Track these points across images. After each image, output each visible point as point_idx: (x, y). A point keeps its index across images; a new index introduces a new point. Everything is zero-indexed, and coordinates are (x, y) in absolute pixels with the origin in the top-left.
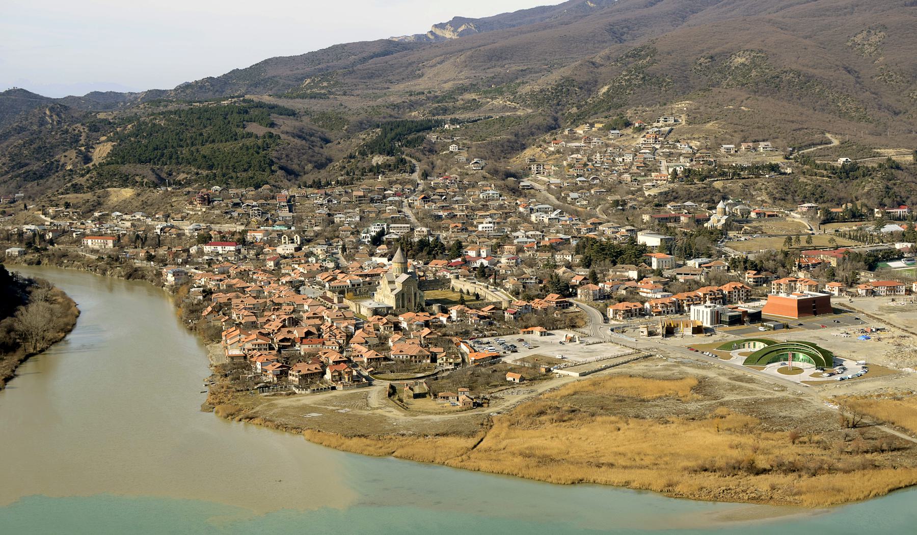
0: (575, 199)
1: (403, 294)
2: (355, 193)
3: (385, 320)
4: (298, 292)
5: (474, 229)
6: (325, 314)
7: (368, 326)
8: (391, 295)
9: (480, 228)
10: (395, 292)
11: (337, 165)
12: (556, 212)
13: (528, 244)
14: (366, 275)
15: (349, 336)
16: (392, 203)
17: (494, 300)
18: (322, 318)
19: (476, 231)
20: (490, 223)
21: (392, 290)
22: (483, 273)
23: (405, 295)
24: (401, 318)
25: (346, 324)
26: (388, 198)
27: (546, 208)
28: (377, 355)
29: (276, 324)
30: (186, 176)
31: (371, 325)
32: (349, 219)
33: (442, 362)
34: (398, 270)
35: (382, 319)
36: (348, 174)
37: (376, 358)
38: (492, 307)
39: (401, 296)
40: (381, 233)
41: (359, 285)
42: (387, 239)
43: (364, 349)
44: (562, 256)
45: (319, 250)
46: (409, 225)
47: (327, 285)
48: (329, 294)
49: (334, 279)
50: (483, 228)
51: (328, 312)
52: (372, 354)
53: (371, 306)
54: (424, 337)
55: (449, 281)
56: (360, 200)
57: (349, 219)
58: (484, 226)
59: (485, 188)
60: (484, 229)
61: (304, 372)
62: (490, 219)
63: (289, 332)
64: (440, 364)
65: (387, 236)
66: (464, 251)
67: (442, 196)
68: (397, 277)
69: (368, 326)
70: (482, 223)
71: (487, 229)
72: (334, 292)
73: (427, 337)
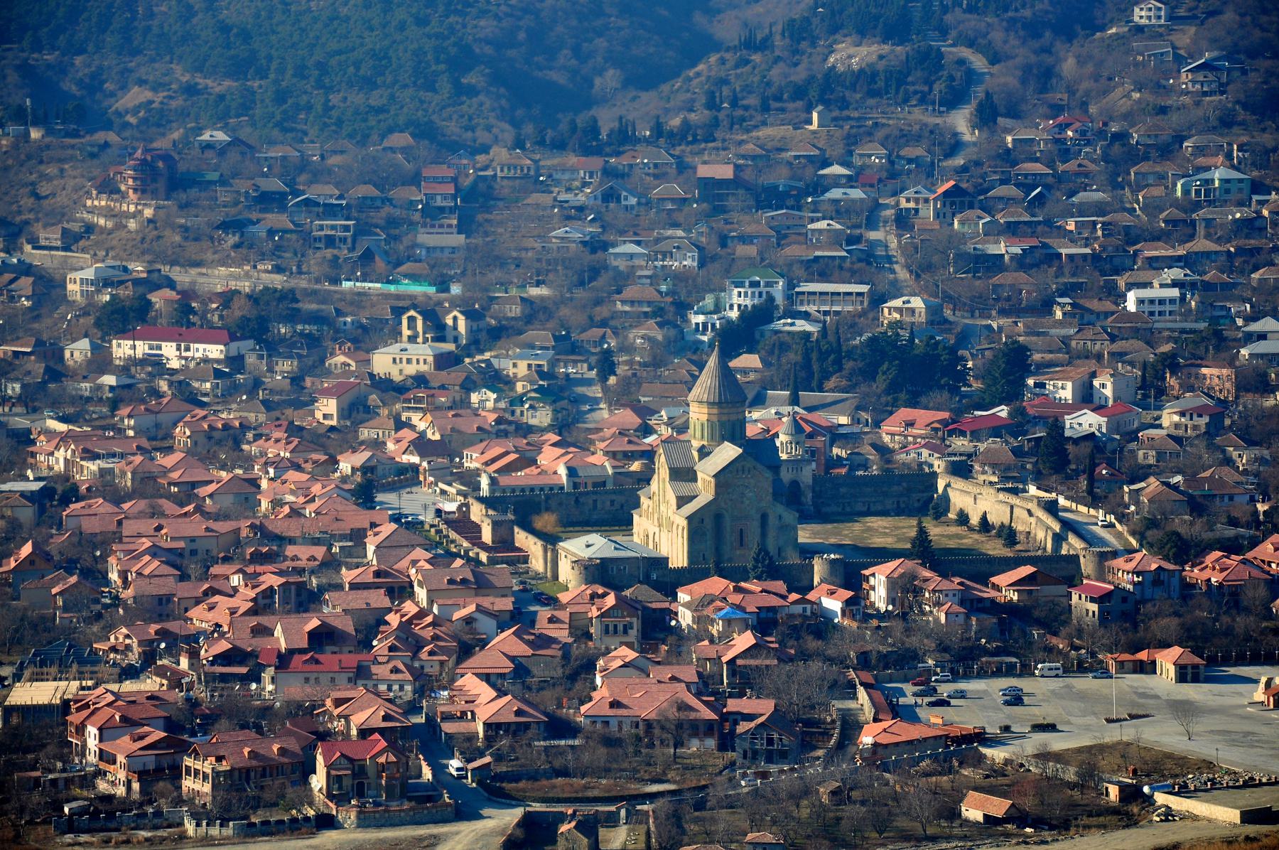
1: (718, 518)
2: (704, 171)
11: (698, 74)
23: (727, 523)
30: (148, 95)
39: (709, 524)
60: (1147, 308)
71: (1157, 308)
73: (739, 662)
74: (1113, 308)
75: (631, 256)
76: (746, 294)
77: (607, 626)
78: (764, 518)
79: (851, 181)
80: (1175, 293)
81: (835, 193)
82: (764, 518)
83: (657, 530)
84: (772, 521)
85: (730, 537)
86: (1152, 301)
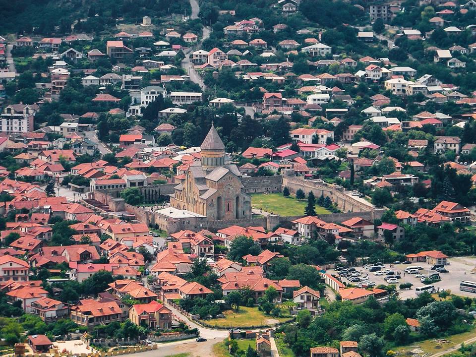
0: (448, 59)
1: (219, 198)
3: (200, 237)
4: (50, 191)
5: (300, 101)
6: (104, 226)
7: (174, 246)
8: (199, 200)
9: (310, 100)
10: (205, 196)
12: (422, 79)
13: (390, 128)
14: (149, 170)
15: (149, 258)
16: (166, 60)
17: (356, 210)
18: (98, 232)
19: (303, 105)
20: (323, 92)
21: (202, 192)
22: (328, 170)
24: (221, 235)
25: (140, 243)
26: (160, 52)
27: (406, 72)
28: (201, 290)
29: (27, 242)
31: (179, 244)
32: (104, 84)
33: (302, 301)
34: (210, 162)
35: (193, 235)
36: (91, 14)
37: (200, 295)
38: (358, 219)
39: (215, 202)
40: (160, 103)
41: (141, 183)
42: (167, 113)
43: (180, 282)
44: (444, 145)
45: (65, 131)
46: (200, 94)
47: (93, 183)
48: (99, 197)
49: (101, 174)
50: (315, 100)
51: (107, 224)
52: (193, 288)
53: (172, 216)
54: (266, 263)
55: (279, 179)
56: (118, 54)
57: (104, 84)
58: (317, 95)
59: (307, 40)
60: (317, 102)
61: (96, 313)
62: (324, 88)
63: (55, 253)
64: (299, 305)
65: (168, 110)
66: (292, 136)
67: (243, 50)
68: (208, 172)
69: (174, 246)
70: (309, 93)
71: (321, 102)
72: (106, 193)
74: (303, 102)
75: (91, 81)
76: (150, 96)
77: (201, 249)
78: (237, 198)
79: (169, 48)
80: (327, 96)
81: (164, 53)
82: (237, 198)
83: (186, 205)
84: (241, 199)
85: (224, 207)
86: (319, 100)
